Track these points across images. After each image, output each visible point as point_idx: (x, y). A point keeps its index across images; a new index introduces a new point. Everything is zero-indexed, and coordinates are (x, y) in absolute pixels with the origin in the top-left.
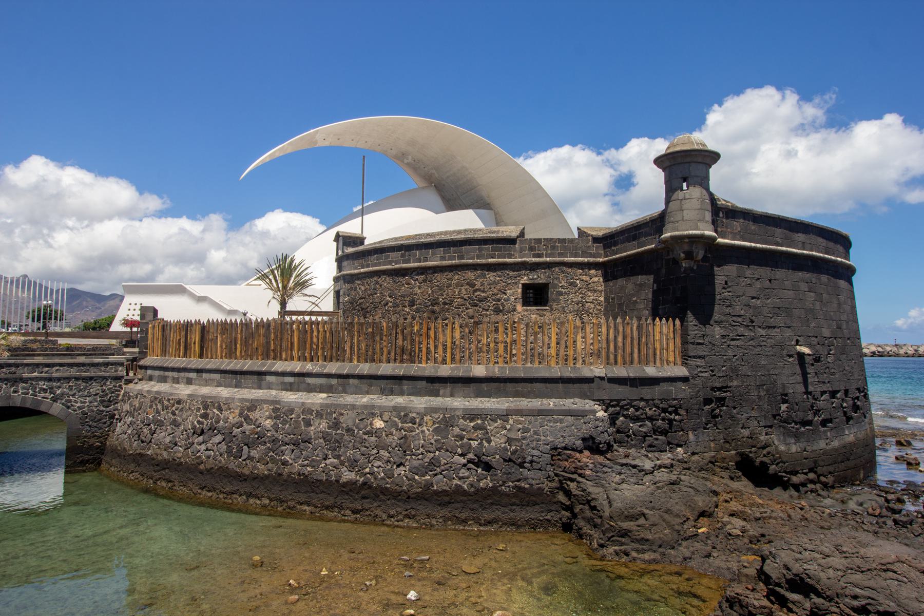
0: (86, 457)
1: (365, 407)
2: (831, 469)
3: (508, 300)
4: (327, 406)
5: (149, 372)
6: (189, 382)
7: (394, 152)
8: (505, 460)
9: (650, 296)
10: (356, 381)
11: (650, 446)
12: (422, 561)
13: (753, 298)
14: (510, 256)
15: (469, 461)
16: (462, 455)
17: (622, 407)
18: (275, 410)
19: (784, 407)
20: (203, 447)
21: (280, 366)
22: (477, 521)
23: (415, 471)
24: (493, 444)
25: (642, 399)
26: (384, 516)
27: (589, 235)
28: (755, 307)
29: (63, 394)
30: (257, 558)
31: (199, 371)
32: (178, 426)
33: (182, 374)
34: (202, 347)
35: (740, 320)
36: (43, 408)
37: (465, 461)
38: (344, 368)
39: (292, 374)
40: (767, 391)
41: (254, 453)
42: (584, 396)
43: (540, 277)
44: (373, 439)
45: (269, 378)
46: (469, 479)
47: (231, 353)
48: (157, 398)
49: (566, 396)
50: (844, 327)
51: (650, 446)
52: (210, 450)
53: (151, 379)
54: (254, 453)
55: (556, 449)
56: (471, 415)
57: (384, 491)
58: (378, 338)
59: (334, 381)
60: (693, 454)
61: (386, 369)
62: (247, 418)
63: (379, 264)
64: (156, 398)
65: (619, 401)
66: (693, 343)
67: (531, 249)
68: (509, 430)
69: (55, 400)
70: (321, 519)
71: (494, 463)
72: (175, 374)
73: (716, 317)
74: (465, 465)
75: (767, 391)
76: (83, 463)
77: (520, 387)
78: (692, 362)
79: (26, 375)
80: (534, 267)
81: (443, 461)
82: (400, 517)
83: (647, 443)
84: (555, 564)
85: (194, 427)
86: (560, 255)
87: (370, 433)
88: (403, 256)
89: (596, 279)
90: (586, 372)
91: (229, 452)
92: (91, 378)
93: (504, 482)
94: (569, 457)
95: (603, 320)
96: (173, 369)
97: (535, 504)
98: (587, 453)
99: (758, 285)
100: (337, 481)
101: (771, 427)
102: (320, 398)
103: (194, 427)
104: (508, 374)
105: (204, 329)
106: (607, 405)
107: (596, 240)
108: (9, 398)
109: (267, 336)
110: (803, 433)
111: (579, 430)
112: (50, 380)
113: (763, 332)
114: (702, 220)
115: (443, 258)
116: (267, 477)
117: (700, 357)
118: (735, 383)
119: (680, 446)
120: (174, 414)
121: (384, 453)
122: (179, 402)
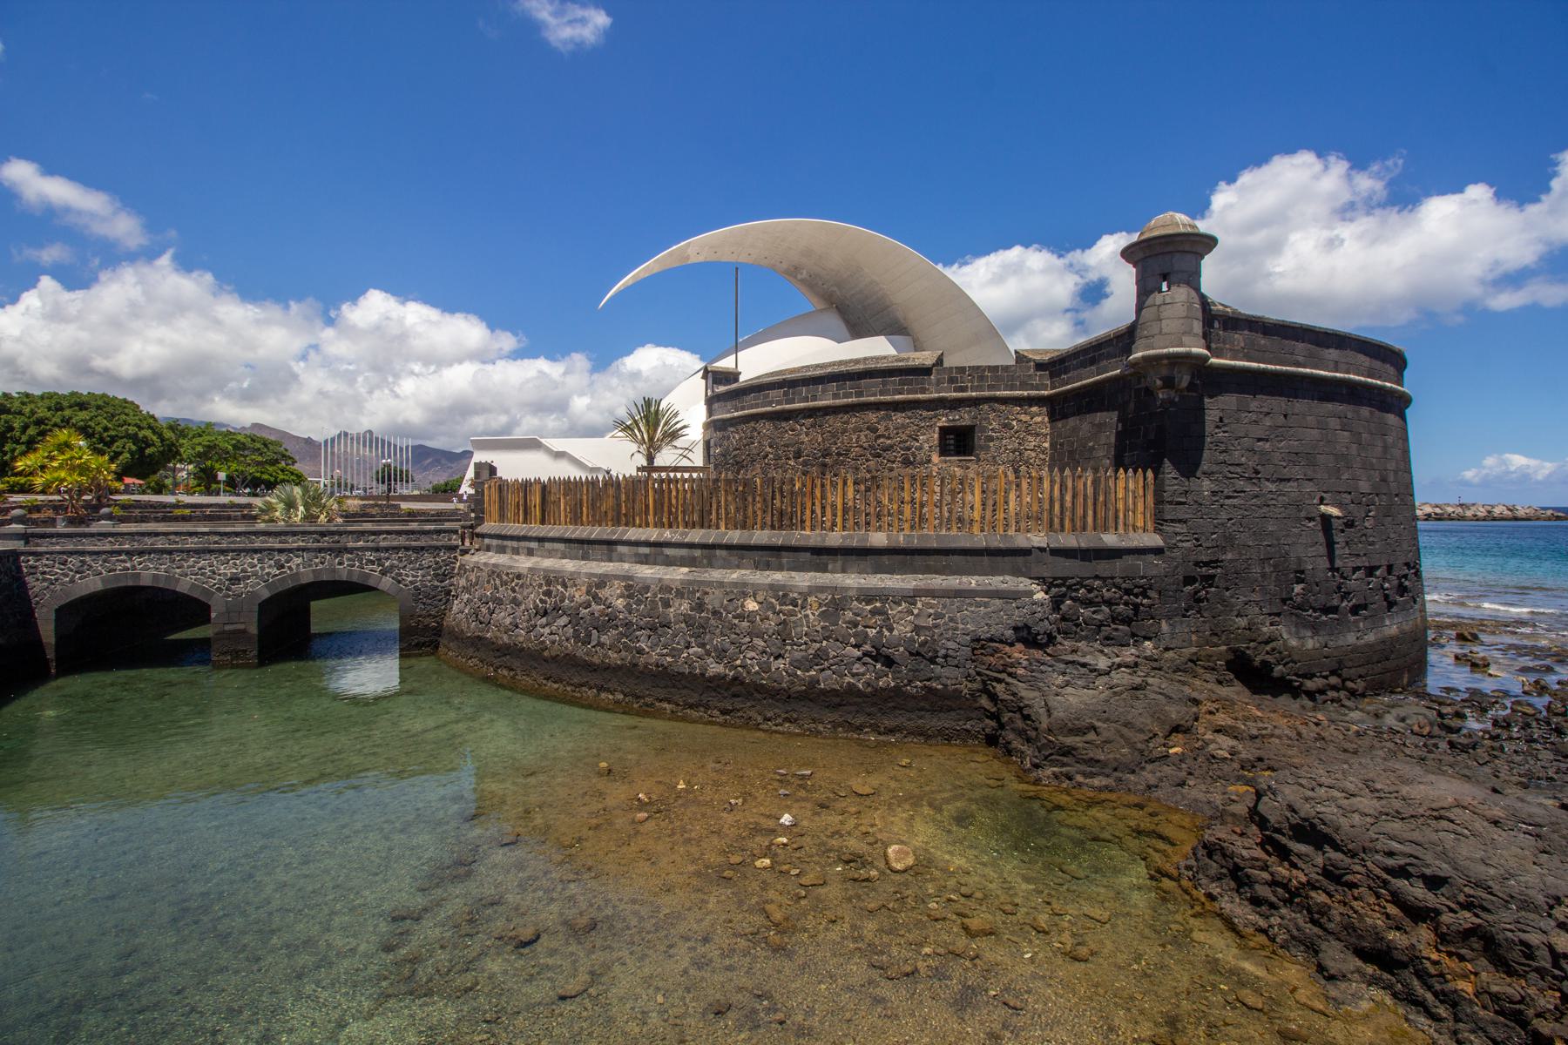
0: (422, 639)
1: (735, 584)
2: (1362, 671)
3: (920, 448)
4: (690, 582)
5: (487, 541)
6: (530, 553)
7: (784, 266)
8: (911, 654)
9: (1113, 440)
10: (724, 553)
11: (1107, 638)
12: (803, 777)
13: (1259, 440)
14: (923, 391)
15: (865, 654)
16: (856, 646)
17: (1069, 587)
18: (628, 587)
19: (1298, 588)
20: (547, 630)
21: (633, 534)
22: (875, 729)
23: (797, 664)
24: (895, 632)
25: (1097, 577)
26: (760, 719)
27: (1030, 360)
28: (1263, 453)
29: (392, 566)
30: (604, 765)
31: (541, 540)
32: (518, 605)
33: (523, 544)
34: (543, 511)
35: (1239, 470)
36: (371, 583)
37: (859, 654)
38: (711, 536)
39: (647, 544)
40: (1275, 566)
41: (604, 638)
42: (1017, 573)
43: (963, 418)
44: (745, 624)
45: (620, 548)
46: (864, 676)
47: (576, 519)
48: (495, 572)
49: (994, 572)
50: (1391, 478)
51: (1107, 638)
52: (554, 634)
53: (488, 549)
54: (604, 638)
55: (978, 640)
56: (867, 596)
57: (759, 688)
58: (750, 499)
59: (697, 553)
60: (1167, 649)
61: (761, 536)
62: (595, 597)
63: (757, 406)
65: (1065, 579)
66: (1171, 503)
67: (952, 380)
68: (917, 616)
69: (383, 573)
70: (684, 719)
71: (897, 657)
72: (515, 544)
73: (1205, 466)
74: (859, 659)
75: (1275, 566)
76: (419, 646)
77: (931, 561)
78: (1167, 528)
79: (350, 545)
80: (955, 405)
81: (832, 654)
82: (779, 720)
83: (1103, 634)
84: (973, 787)
85: (536, 607)
86: (991, 388)
87: (741, 617)
88: (786, 394)
89: (1039, 419)
90: (1021, 541)
91: (576, 636)
92: (422, 548)
93: (910, 682)
94: (996, 651)
95: (1045, 473)
96: (512, 538)
97: (950, 709)
98: (1019, 646)
99: (1268, 422)
100: (703, 675)
101: (1278, 615)
102: (680, 574)
103: (536, 607)
104: (916, 543)
105: (545, 489)
106: (1048, 584)
107: (1040, 366)
108: (334, 571)
109: (617, 498)
110: (1324, 623)
111: (1010, 616)
112: (377, 550)
113: (1273, 487)
114: (1188, 332)
115: (836, 396)
116: (620, 667)
117: (1180, 521)
118: (1229, 556)
119: (1149, 639)
120: (514, 591)
121: (759, 642)
122: (519, 576)
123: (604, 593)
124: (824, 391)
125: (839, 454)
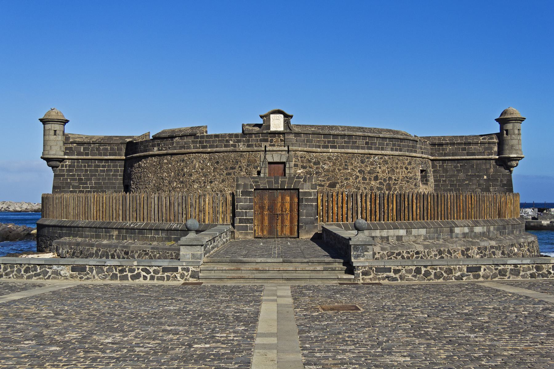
14: (415, 152)
18: (479, 249)
34: (399, 211)
62: (468, 257)
64: (393, 253)
88: (367, 143)
115: (392, 150)
123: (470, 253)
124: (387, 145)
125: (395, 180)
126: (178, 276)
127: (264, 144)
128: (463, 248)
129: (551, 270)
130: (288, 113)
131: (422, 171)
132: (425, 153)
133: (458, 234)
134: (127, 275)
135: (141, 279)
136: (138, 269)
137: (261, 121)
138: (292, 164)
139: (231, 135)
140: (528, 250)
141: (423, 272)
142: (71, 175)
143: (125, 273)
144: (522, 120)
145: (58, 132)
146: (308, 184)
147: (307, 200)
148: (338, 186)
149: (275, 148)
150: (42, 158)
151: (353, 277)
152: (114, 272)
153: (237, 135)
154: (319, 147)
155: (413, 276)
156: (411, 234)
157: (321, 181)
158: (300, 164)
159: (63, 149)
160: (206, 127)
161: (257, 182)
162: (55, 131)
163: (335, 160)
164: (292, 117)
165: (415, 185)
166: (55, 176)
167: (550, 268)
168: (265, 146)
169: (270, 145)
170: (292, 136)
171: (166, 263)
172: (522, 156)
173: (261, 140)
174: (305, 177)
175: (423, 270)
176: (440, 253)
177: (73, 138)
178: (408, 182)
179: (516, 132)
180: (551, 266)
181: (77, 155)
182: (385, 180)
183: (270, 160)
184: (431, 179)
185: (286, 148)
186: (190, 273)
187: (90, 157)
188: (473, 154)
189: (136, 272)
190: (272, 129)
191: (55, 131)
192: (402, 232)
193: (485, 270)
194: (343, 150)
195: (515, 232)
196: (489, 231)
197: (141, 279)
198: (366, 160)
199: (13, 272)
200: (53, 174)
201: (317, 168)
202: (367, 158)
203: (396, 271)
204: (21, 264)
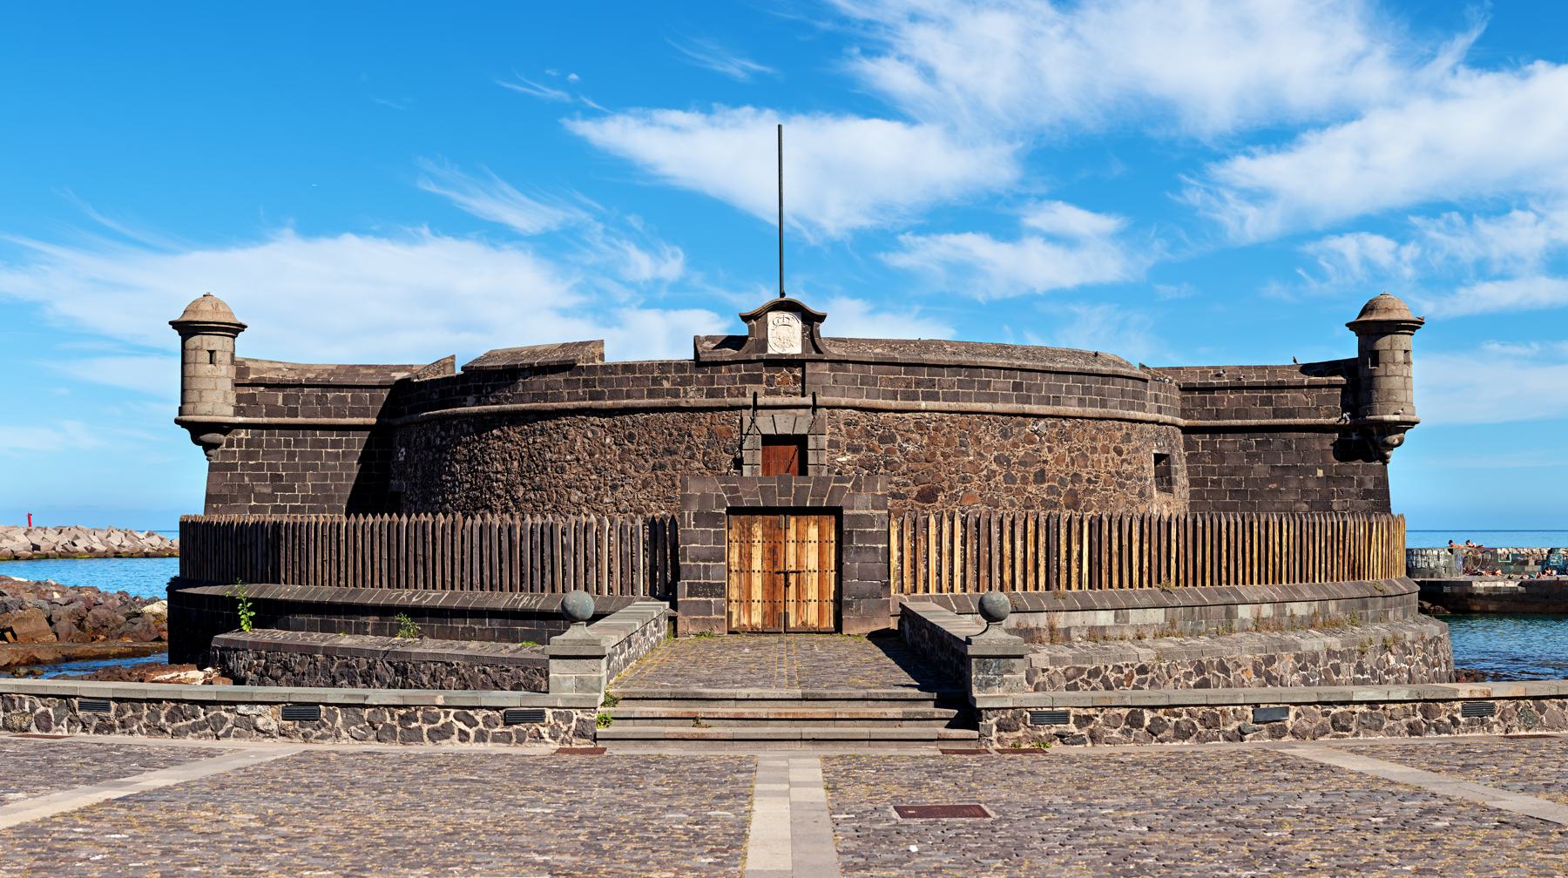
14: (1142, 408)
18: (1298, 658)
62: (1271, 679)
64: (1080, 671)
115: (1081, 402)
123: (1277, 668)
124: (1069, 390)
125: (1089, 481)
126: (545, 731)
127: (750, 388)
128: (1259, 656)
129: (1458, 716)
130: (814, 307)
131: (1159, 458)
132: (1168, 411)
133: (1244, 621)
134: (420, 728)
135: (455, 737)
136: (447, 714)
137: (742, 330)
138: (824, 440)
139: (664, 366)
140: (1424, 660)
141: (1147, 722)
142: (252, 467)
143: (414, 725)
144: (1411, 326)
145: (218, 355)
146: (865, 496)
147: (863, 536)
148: (941, 497)
149: (779, 400)
150: (177, 422)
151: (975, 734)
152: (388, 721)
153: (680, 366)
154: (894, 397)
155: (1122, 732)
156: (1127, 622)
157: (897, 484)
158: (843, 440)
159: (232, 399)
160: (601, 343)
161: (735, 490)
162: (212, 352)
163: (935, 429)
164: (821, 318)
165: (1141, 494)
166: (212, 468)
167: (1456, 711)
168: (755, 395)
169: (767, 393)
170: (823, 368)
171: (512, 699)
172: (1412, 419)
173: (743, 380)
174: (858, 478)
175: (1148, 716)
176: (1200, 669)
177: (258, 371)
178: (1121, 485)
179: (1400, 357)
180: (1458, 705)
181: (267, 415)
182: (1062, 482)
183: (769, 431)
184: (1182, 479)
185: (808, 400)
186: (574, 724)
187: (300, 420)
188: (1291, 413)
189: (442, 721)
190: (774, 349)
191: (212, 352)
192: (1104, 618)
193: (1298, 716)
194: (954, 405)
195: (1391, 614)
196: (1325, 611)
197: (455, 737)
198: (1016, 430)
199: (140, 718)
200: (205, 464)
201: (887, 451)
202: (1018, 424)
203: (1081, 721)
204: (159, 701)
